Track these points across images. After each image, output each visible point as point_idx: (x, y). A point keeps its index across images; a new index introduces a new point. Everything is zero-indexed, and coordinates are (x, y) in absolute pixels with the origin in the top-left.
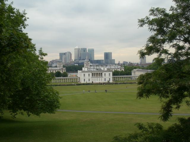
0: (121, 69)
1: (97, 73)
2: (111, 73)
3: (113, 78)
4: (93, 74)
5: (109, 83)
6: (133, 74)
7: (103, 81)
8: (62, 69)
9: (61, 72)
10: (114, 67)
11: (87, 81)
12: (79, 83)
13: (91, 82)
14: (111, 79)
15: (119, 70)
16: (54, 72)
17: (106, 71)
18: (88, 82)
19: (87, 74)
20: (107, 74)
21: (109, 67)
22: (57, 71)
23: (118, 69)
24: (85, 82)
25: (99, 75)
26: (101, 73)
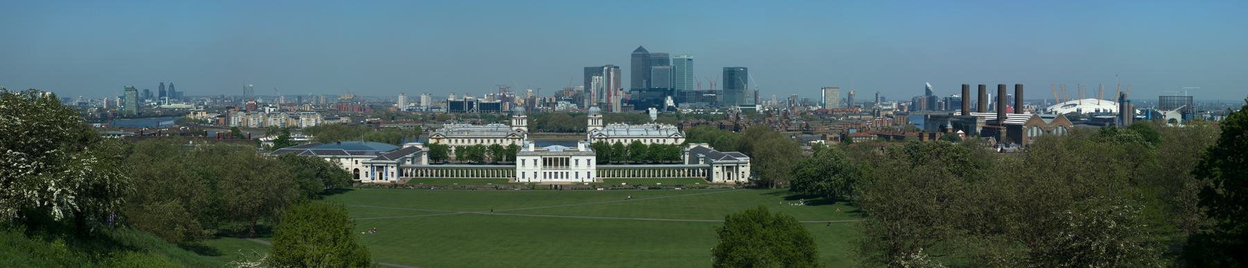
0: (676, 139)
1: (556, 160)
2: (593, 159)
3: (598, 170)
4: (545, 160)
5: (578, 188)
7: (572, 179)
9: (506, 143)
13: (540, 179)
14: (594, 174)
15: (670, 142)
17: (581, 154)
18: (533, 180)
22: (492, 142)
24: (526, 180)
26: (567, 160)
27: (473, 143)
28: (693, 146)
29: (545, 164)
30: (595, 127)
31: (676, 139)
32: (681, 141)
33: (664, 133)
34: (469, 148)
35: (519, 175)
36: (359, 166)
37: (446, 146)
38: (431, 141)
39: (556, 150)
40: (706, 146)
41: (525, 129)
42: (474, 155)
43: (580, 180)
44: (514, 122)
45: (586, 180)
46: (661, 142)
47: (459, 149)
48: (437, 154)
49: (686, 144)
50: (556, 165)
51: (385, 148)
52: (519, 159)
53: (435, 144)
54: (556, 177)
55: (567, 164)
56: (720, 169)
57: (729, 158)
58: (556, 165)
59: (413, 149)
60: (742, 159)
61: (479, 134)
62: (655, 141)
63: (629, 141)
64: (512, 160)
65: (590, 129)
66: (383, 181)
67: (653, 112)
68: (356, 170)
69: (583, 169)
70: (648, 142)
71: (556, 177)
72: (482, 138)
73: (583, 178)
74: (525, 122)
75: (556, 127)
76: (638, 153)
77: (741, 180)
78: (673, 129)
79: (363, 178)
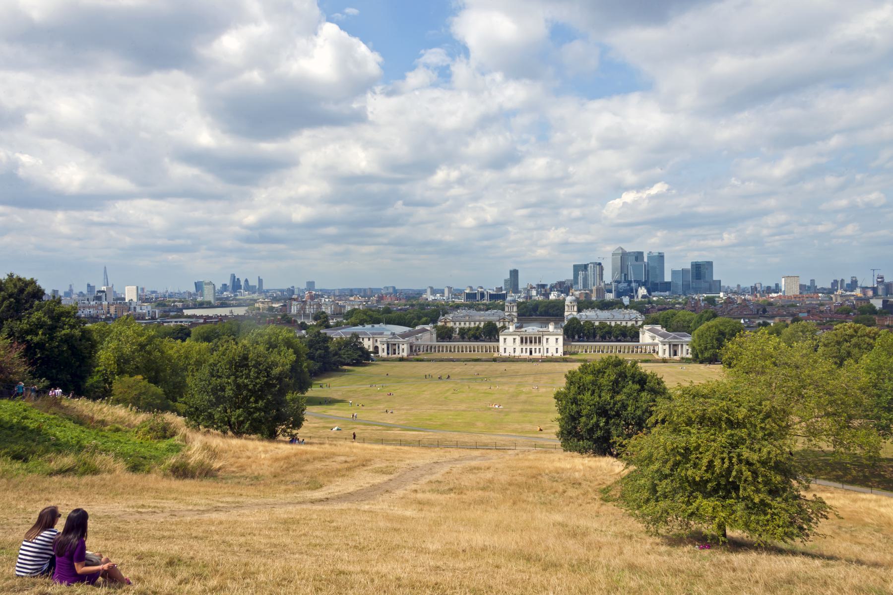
2: (561, 338)
4: (522, 339)
6: (641, 335)
8: (504, 319)
10: (621, 317)
11: (509, 352)
12: (496, 355)
13: (518, 353)
14: (561, 350)
16: (482, 324)
19: (510, 339)
20: (552, 339)
21: (611, 317)
23: (631, 320)
24: (507, 354)
25: (535, 342)
26: (540, 338)
27: (472, 325)
28: (646, 327)
29: (522, 342)
30: (570, 313)
31: (637, 322)
32: (640, 323)
33: (627, 317)
34: (469, 329)
35: (501, 350)
36: (378, 344)
37: (452, 327)
38: (439, 324)
39: (532, 329)
40: (659, 327)
41: (515, 314)
42: (474, 335)
43: (550, 354)
44: (506, 309)
45: (555, 355)
46: (624, 324)
47: (461, 329)
48: (445, 335)
49: (641, 326)
50: (531, 342)
51: (400, 329)
52: (501, 338)
53: (443, 327)
54: (531, 353)
55: (540, 342)
56: (667, 347)
57: (675, 338)
58: (531, 342)
59: (424, 330)
60: (687, 339)
61: (478, 318)
62: (619, 323)
63: (597, 323)
64: (498, 341)
65: (566, 314)
66: (396, 356)
67: (626, 300)
68: (376, 348)
69: (553, 343)
70: (613, 324)
71: (531, 353)
72: (480, 321)
73: (552, 352)
74: (515, 309)
75: (539, 311)
76: (607, 334)
77: (684, 355)
78: (635, 313)
79: (380, 353)
